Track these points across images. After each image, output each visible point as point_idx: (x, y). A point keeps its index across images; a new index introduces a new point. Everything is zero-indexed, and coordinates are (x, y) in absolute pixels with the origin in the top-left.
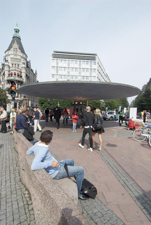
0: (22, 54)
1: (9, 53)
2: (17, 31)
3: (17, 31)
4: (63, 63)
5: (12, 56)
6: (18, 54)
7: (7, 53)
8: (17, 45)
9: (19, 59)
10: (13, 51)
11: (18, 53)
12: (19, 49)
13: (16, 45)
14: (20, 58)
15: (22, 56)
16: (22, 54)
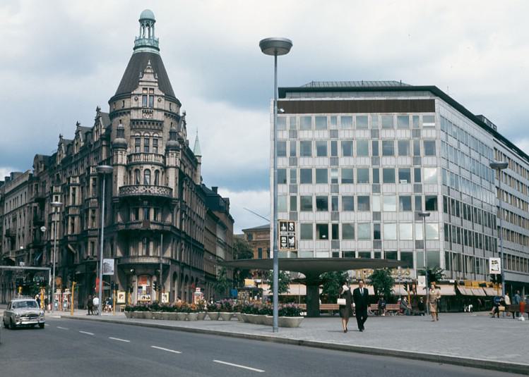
0: (168, 103)
1: (127, 106)
2: (147, 22)
3: (147, 22)
4: (313, 130)
5: (136, 115)
6: (155, 107)
7: (119, 105)
8: (152, 76)
9: (161, 123)
10: (140, 98)
11: (156, 102)
12: (160, 89)
13: (149, 77)
14: (158, 116)
15: (168, 109)
16: (164, 105)
